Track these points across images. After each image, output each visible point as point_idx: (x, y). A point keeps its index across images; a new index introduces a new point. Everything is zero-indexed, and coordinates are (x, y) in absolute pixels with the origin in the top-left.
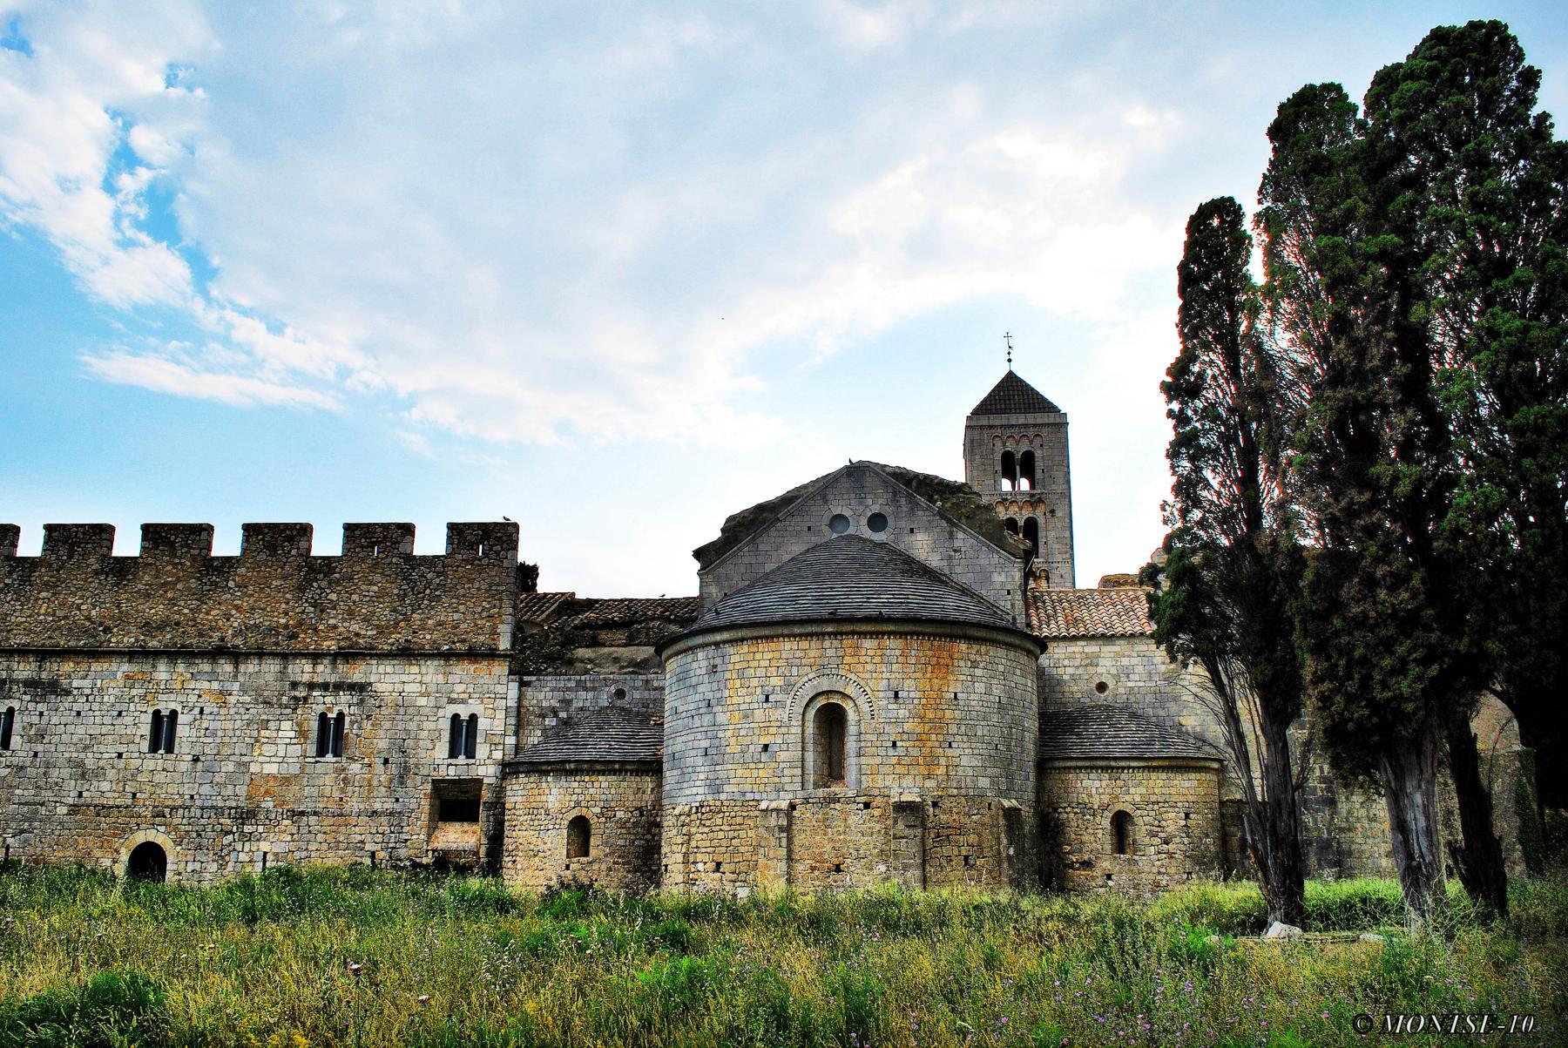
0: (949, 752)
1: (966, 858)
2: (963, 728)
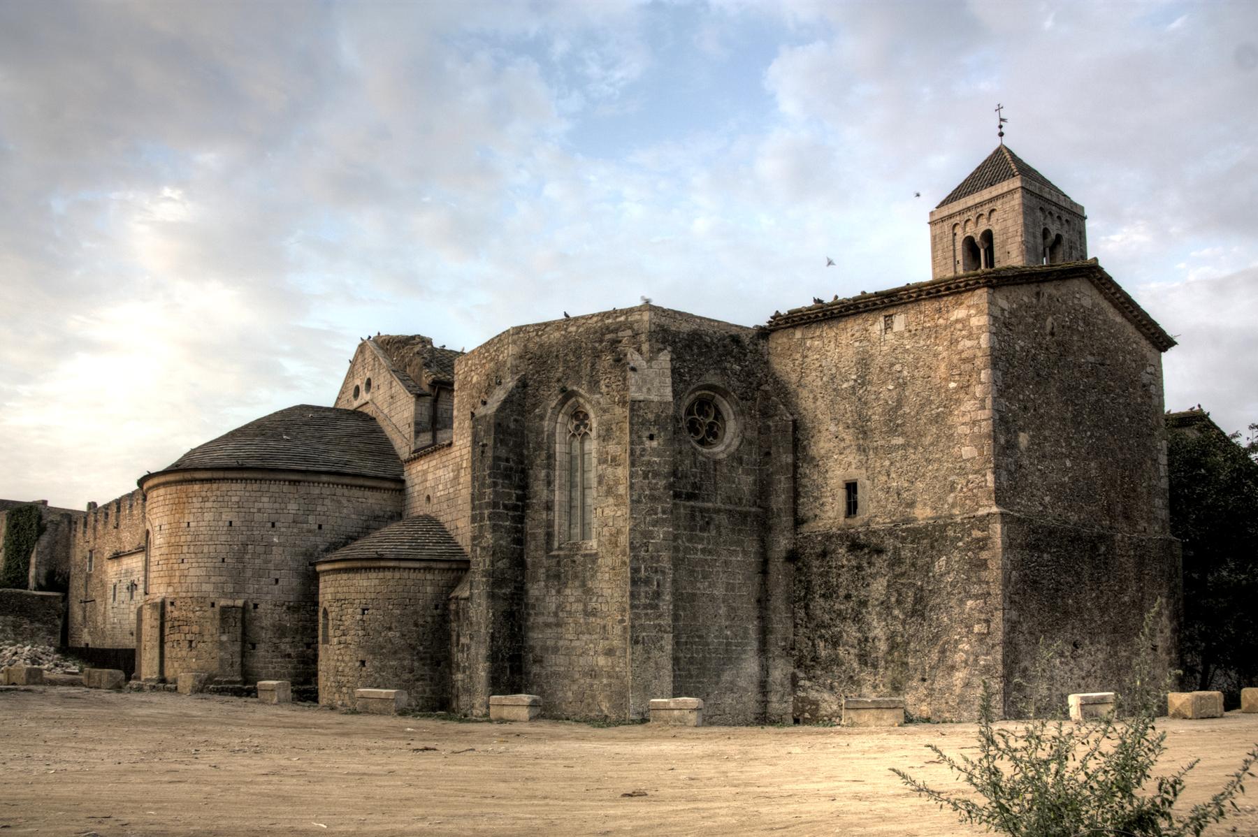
0: (182, 566)
1: (191, 642)
2: (192, 547)
